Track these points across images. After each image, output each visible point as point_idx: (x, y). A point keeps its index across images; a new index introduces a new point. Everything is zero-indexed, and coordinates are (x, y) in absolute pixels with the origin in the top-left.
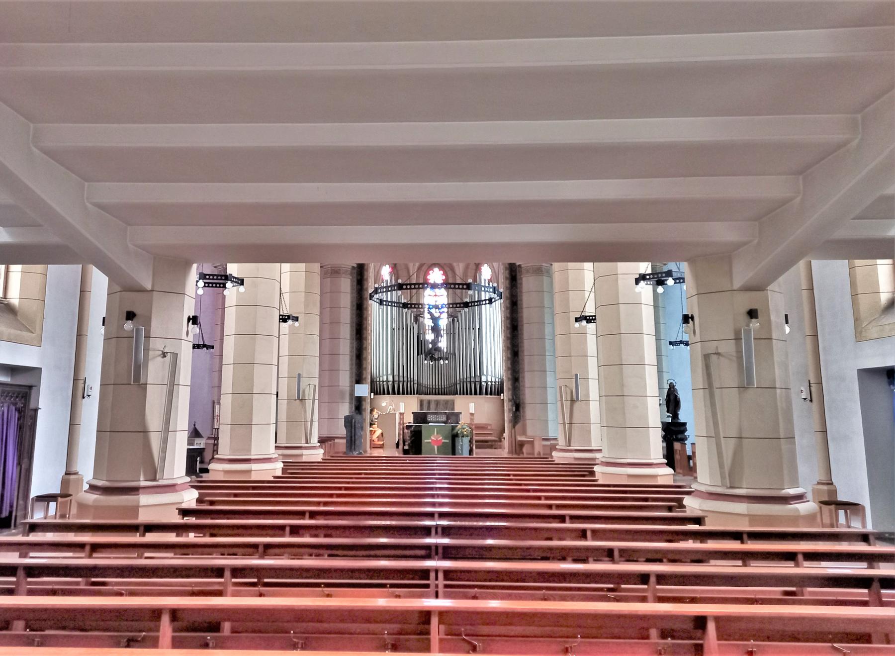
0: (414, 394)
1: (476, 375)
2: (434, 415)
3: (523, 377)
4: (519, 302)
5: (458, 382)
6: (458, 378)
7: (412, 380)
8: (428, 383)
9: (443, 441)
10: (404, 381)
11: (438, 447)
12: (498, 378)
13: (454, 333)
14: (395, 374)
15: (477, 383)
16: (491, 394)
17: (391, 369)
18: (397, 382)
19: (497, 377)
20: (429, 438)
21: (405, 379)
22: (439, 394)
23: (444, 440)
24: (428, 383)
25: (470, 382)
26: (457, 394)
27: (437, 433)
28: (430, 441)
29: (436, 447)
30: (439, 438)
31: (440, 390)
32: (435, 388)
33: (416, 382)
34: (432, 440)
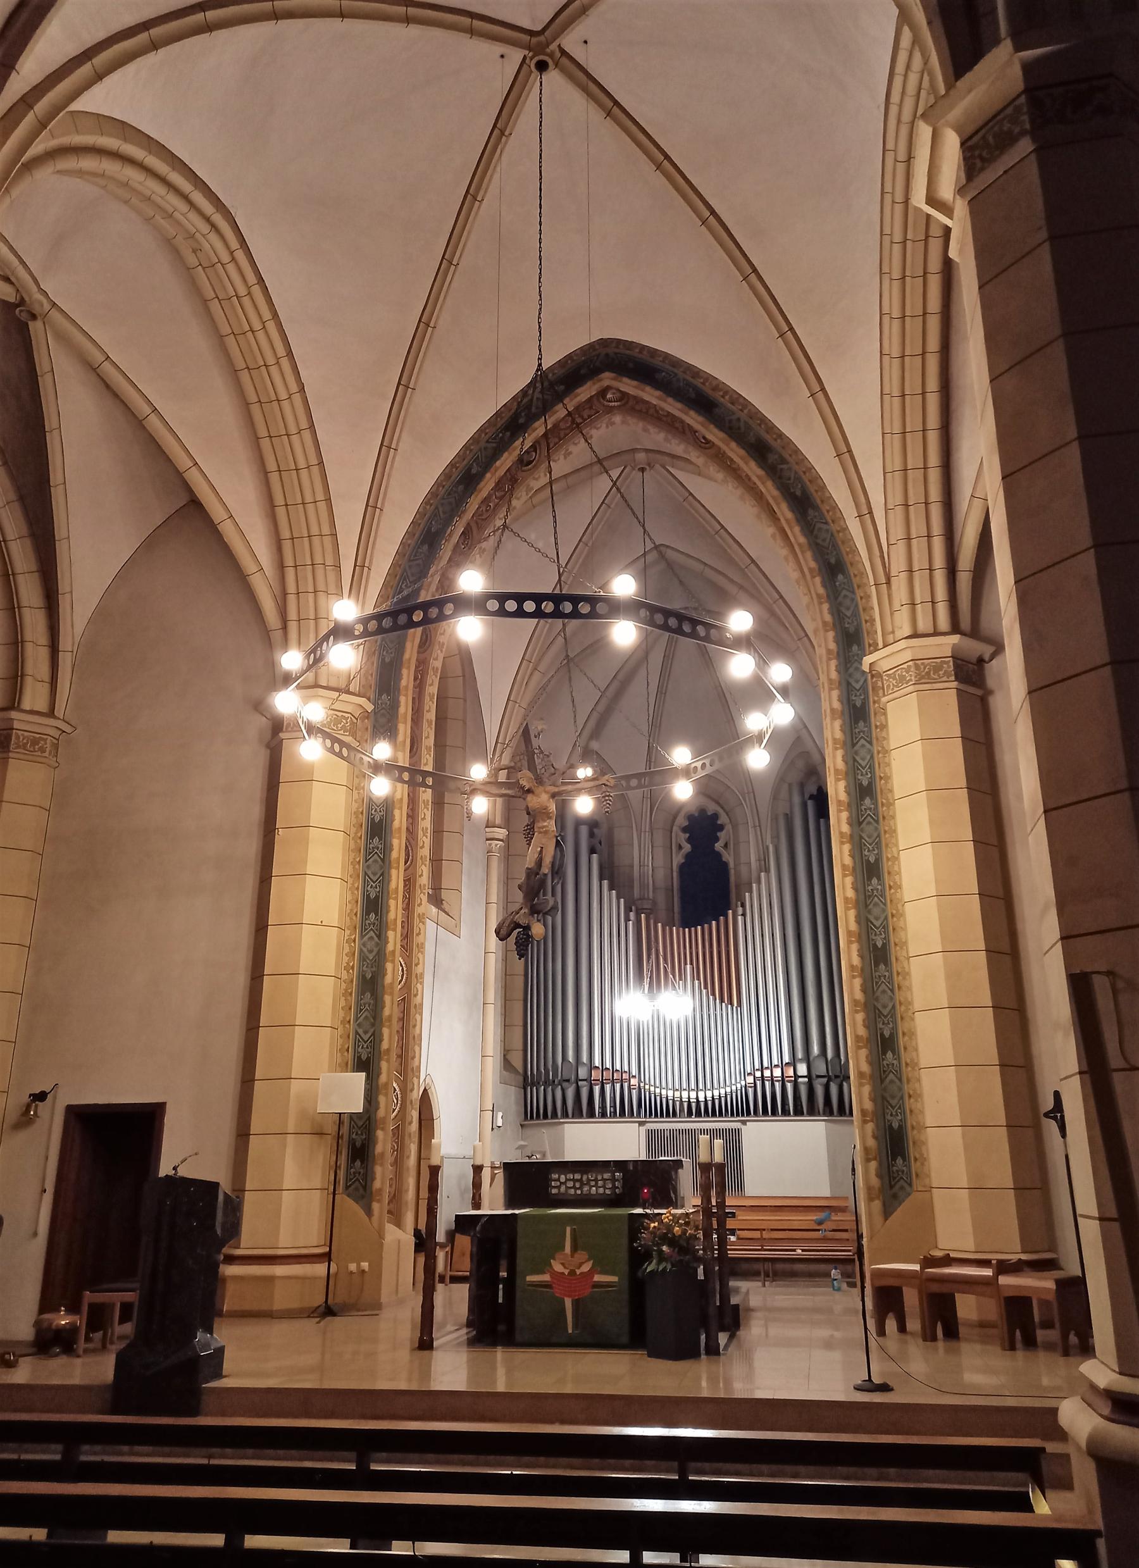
2: (574, 1172)
3: (912, 1034)
4: (880, 784)
9: (597, 1278)
11: (576, 1304)
20: (542, 1266)
23: (600, 1273)
26: (749, 1114)
27: (575, 1248)
28: (546, 1277)
29: (568, 1303)
30: (580, 1266)
34: (554, 1274)
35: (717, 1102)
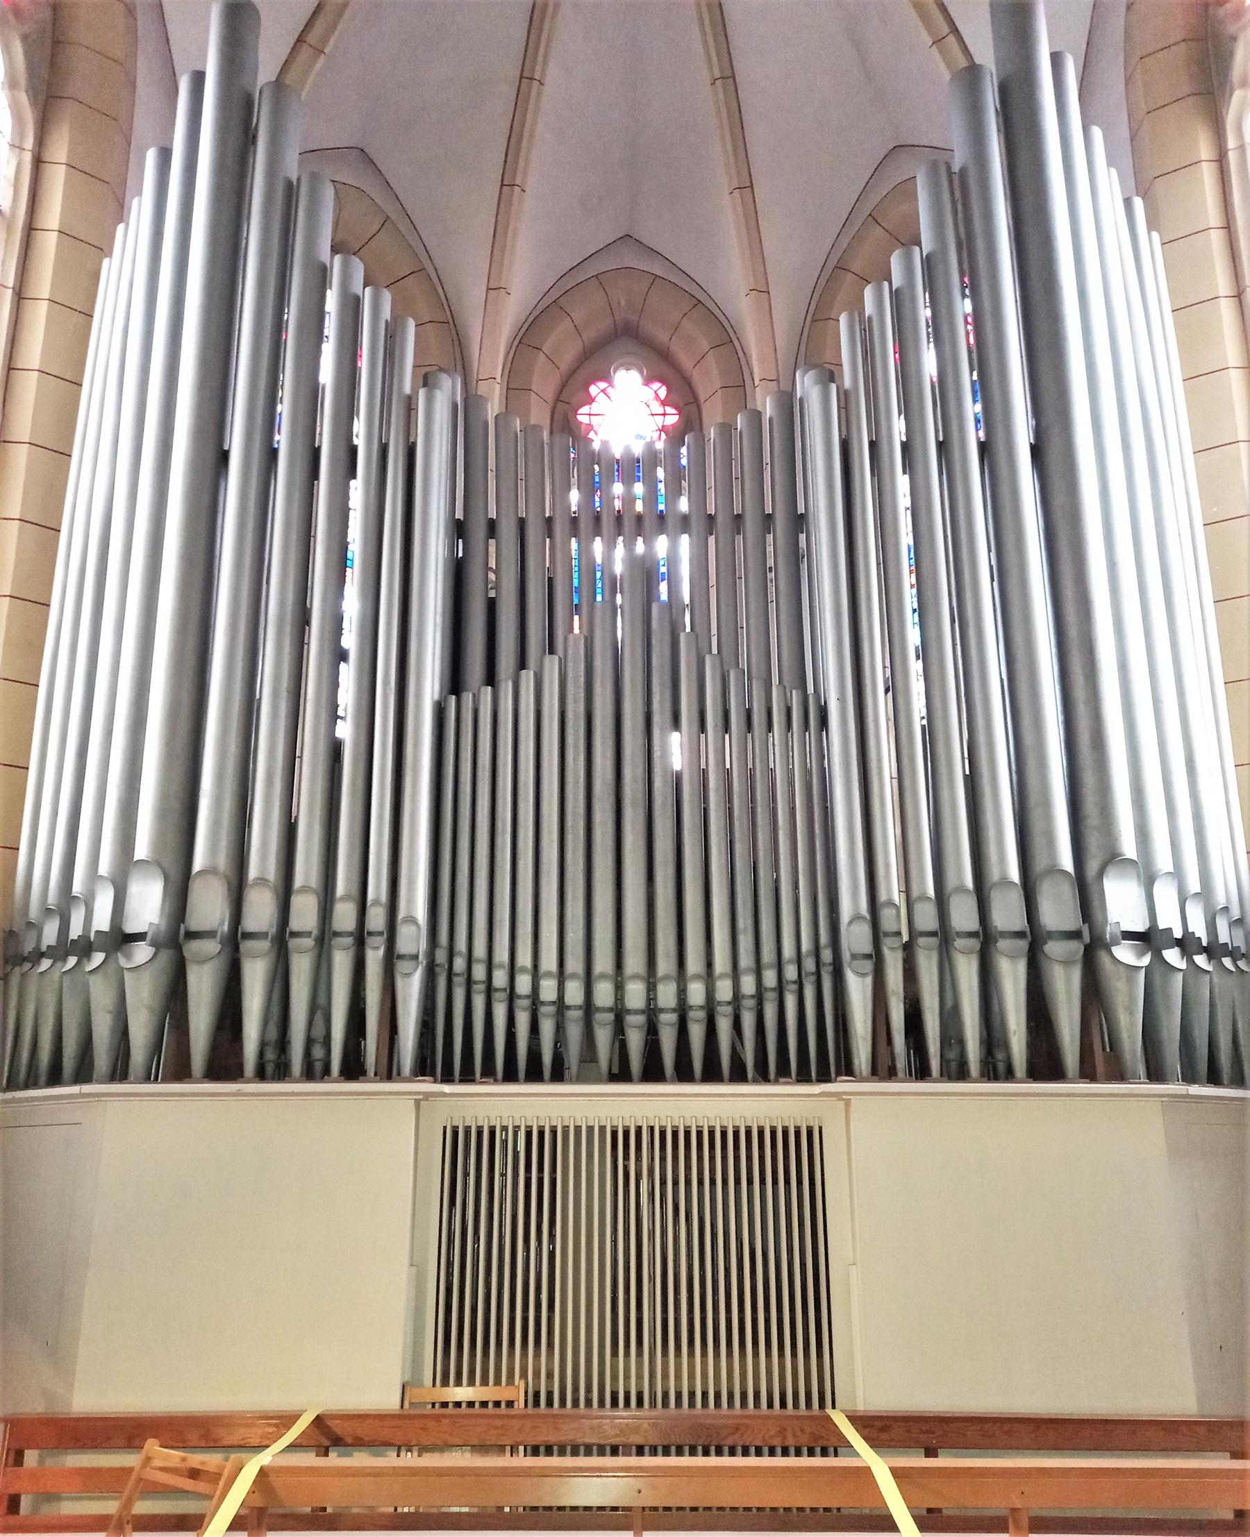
0: (389, 1072)
1: (1040, 863)
5: (856, 938)
6: (852, 901)
7: (377, 918)
8: (549, 961)
10: (282, 938)
12: (1226, 909)
13: (800, 522)
14: (198, 863)
15: (1054, 948)
16: (1189, 1077)
17: (162, 814)
18: (211, 947)
19: (1221, 901)
21: (305, 913)
22: (653, 1073)
24: (549, 961)
25: (986, 938)
31: (668, 1020)
32: (619, 1013)
33: (412, 939)
35: (724, 1026)
